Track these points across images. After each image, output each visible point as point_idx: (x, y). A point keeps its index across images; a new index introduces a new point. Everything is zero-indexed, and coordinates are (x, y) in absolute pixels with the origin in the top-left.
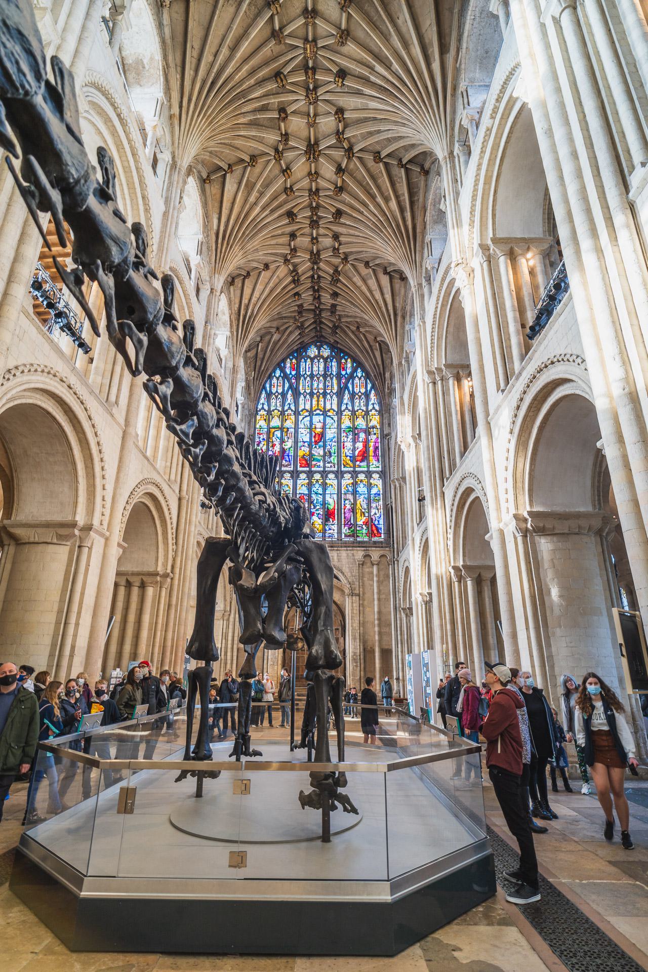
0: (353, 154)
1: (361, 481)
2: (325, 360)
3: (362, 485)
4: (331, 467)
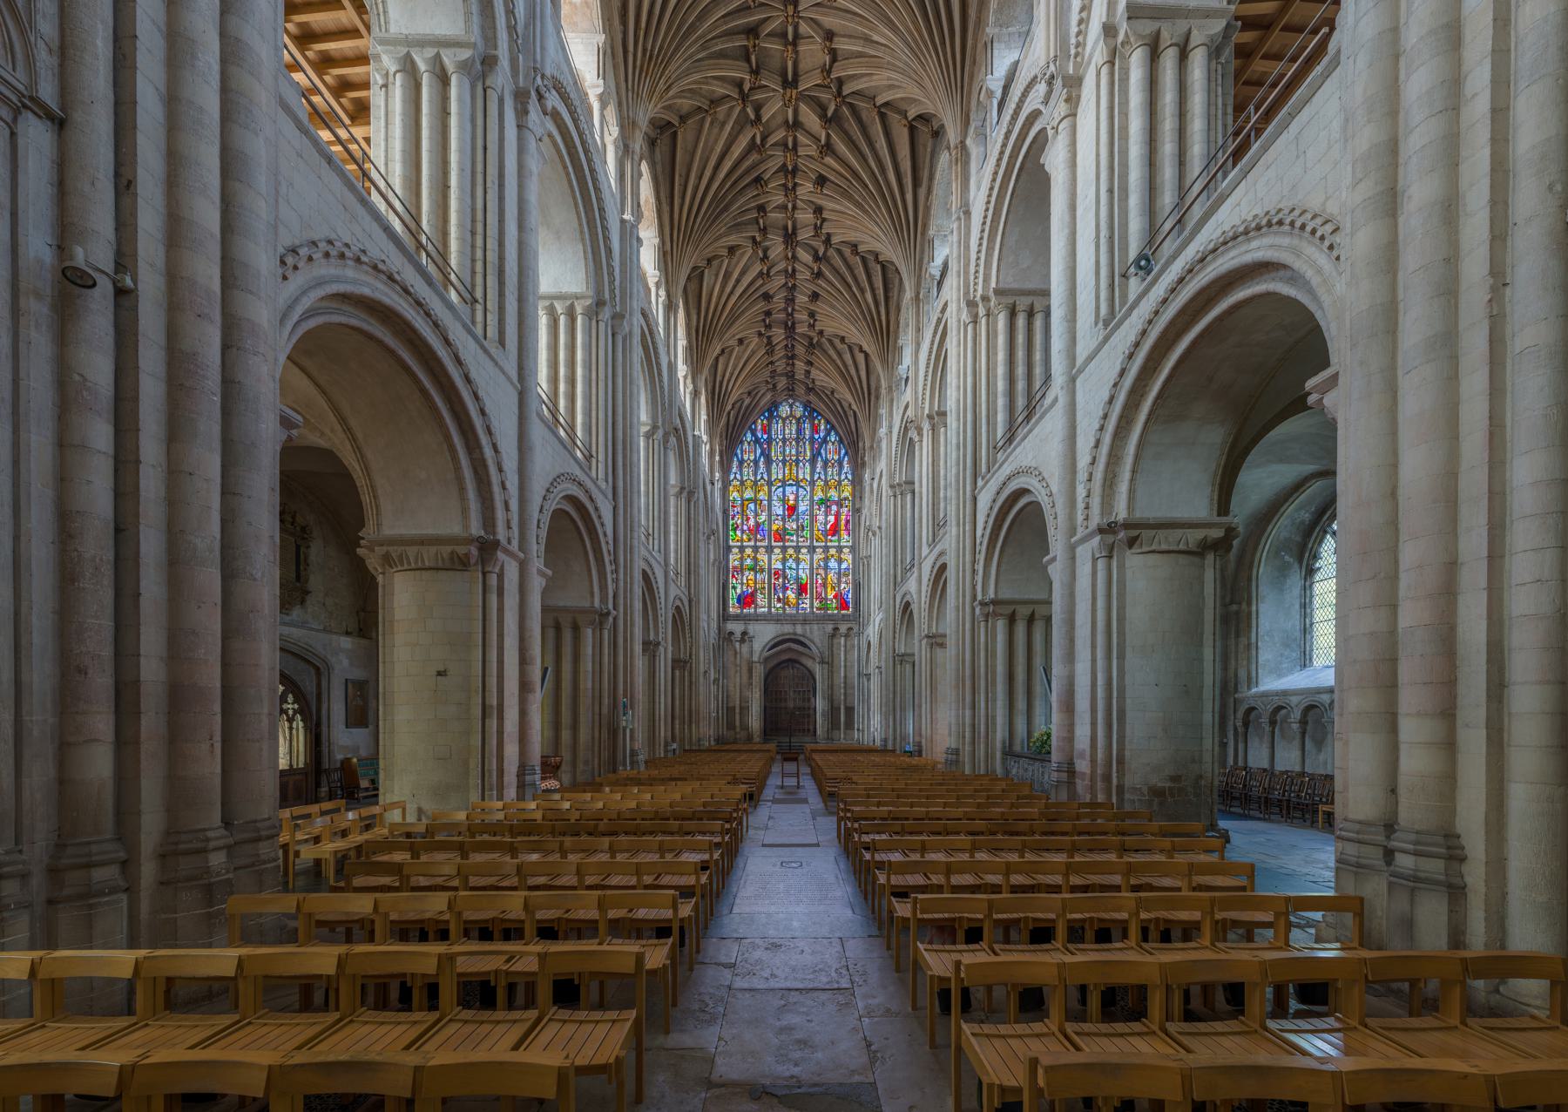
0: (831, 245)
1: (832, 556)
2: (798, 421)
3: (833, 560)
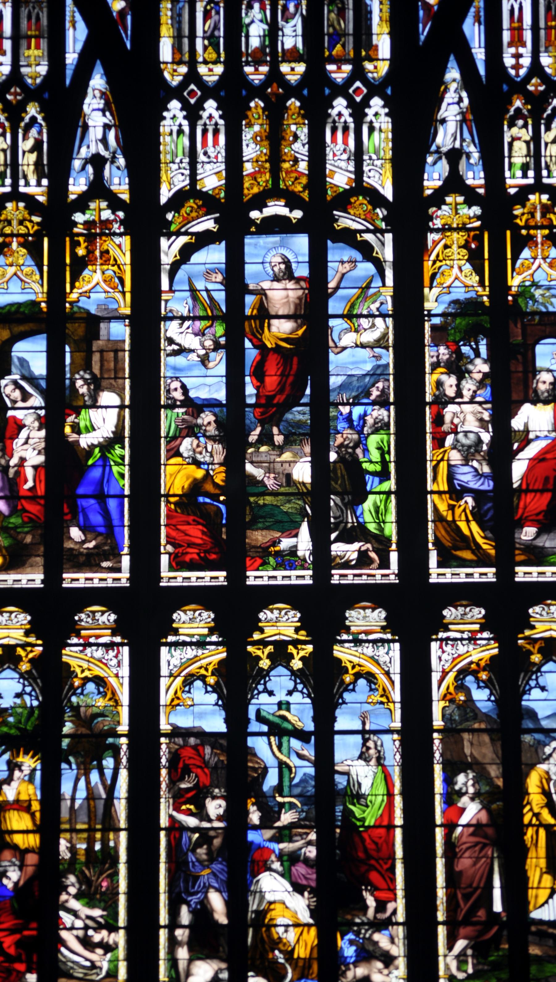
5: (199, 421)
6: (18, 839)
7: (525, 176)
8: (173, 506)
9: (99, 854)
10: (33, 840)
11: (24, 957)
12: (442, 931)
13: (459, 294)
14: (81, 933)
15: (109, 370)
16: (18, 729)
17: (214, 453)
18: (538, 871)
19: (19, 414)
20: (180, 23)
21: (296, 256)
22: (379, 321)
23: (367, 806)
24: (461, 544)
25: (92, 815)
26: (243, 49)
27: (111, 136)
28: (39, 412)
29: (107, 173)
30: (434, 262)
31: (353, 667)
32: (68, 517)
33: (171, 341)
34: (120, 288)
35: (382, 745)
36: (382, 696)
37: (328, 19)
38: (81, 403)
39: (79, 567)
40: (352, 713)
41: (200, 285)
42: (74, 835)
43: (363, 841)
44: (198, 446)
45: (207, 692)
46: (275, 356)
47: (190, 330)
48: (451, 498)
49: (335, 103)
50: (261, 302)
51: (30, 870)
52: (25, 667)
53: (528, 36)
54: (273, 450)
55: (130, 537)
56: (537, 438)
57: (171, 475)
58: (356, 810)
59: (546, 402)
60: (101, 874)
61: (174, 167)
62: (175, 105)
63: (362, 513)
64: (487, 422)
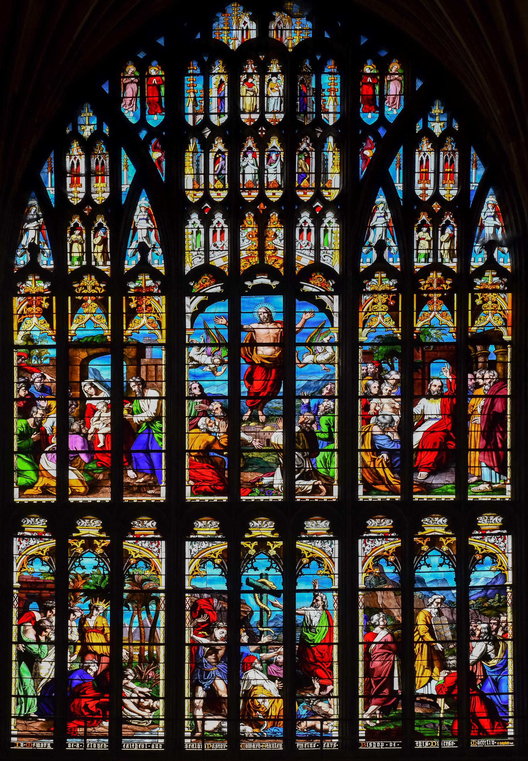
4: (316, 490)
5: (211, 407)
6: (96, 648)
7: (426, 260)
8: (193, 458)
9: (147, 658)
10: (106, 649)
11: (101, 713)
12: (361, 701)
13: (382, 332)
14: (136, 701)
15: (152, 377)
16: (95, 586)
17: (220, 426)
18: (422, 667)
19: (94, 403)
20: (198, 165)
21: (275, 308)
22: (329, 349)
23: (316, 633)
24: (379, 482)
25: (143, 636)
26: (241, 182)
27: (152, 235)
28: (107, 401)
29: (149, 258)
30: (366, 313)
31: (309, 554)
32: (127, 464)
33: (192, 359)
34: (159, 327)
35: (326, 599)
36: (326, 571)
37: (298, 164)
38: (134, 396)
39: (133, 493)
40: (307, 581)
41: (211, 326)
42: (131, 647)
43: (313, 652)
44: (210, 422)
45: (215, 568)
46: (261, 368)
47: (205, 353)
48: (373, 454)
49: (302, 215)
50: (252, 337)
51: (104, 666)
52: (99, 551)
53: (431, 177)
54: (259, 425)
55: (166, 476)
56: (430, 419)
57: (192, 439)
58: (309, 636)
59: (436, 397)
60: (148, 669)
61: (196, 253)
62: (195, 217)
63: (316, 463)
64: (398, 409)
